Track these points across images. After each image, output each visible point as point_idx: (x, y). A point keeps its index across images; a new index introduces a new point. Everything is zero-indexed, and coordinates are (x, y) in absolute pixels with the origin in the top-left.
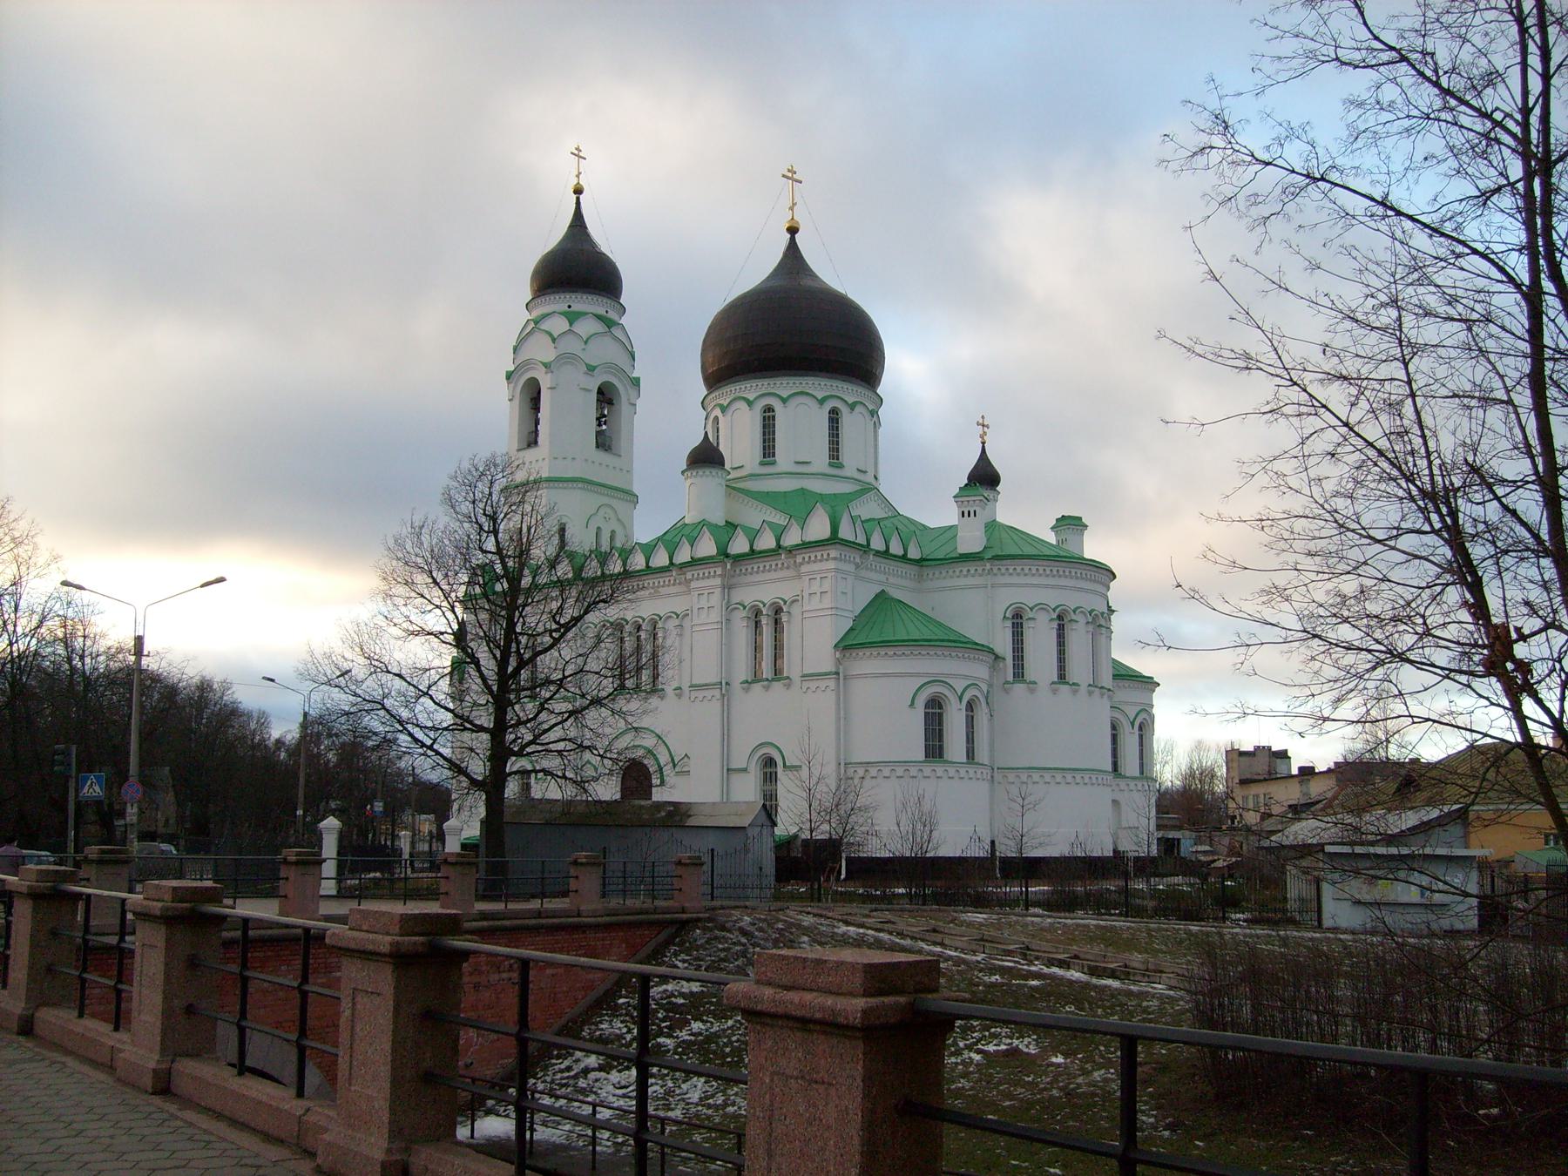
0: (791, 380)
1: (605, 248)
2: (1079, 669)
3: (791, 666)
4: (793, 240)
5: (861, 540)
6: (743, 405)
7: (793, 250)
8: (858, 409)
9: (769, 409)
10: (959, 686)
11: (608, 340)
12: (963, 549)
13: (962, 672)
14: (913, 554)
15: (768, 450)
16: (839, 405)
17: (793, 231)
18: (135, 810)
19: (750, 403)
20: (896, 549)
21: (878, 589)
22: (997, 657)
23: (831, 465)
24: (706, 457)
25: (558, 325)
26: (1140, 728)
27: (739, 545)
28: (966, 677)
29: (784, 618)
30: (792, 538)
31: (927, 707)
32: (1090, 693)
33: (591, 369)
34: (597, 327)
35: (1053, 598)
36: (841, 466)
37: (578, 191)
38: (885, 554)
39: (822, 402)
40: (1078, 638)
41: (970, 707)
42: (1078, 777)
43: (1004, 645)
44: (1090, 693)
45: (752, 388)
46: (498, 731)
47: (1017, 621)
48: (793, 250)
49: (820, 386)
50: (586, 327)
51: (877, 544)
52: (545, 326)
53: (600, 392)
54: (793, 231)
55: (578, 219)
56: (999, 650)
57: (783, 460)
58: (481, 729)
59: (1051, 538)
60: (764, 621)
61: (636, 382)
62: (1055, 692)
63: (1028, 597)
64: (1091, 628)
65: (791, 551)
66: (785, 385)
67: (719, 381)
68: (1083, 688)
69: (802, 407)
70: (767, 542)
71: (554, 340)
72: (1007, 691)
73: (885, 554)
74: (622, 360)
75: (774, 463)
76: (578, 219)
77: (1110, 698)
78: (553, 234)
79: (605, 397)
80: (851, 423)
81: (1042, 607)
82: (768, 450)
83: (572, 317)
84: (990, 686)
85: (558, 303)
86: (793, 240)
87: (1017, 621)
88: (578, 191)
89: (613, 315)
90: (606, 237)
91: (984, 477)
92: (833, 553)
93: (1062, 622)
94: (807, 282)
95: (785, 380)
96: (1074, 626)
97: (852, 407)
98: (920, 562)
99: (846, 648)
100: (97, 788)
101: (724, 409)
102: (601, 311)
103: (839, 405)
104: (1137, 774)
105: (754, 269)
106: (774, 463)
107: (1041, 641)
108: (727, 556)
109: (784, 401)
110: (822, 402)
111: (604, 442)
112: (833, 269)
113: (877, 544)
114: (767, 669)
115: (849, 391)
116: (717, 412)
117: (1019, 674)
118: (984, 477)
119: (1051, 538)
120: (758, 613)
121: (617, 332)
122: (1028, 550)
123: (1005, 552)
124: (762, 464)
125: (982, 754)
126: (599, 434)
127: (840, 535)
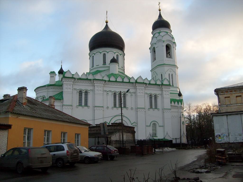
4: (107, 24)
6: (99, 53)
7: (107, 25)
8: (122, 55)
9: (104, 54)
16: (118, 54)
17: (107, 22)
19: (100, 53)
45: (101, 50)
48: (107, 25)
54: (107, 22)
66: (108, 49)
67: (94, 49)
69: (111, 53)
75: (106, 65)
86: (107, 24)
95: (108, 48)
97: (121, 55)
101: (95, 54)
103: (118, 54)
106: (106, 65)
116: (93, 55)
124: (103, 65)
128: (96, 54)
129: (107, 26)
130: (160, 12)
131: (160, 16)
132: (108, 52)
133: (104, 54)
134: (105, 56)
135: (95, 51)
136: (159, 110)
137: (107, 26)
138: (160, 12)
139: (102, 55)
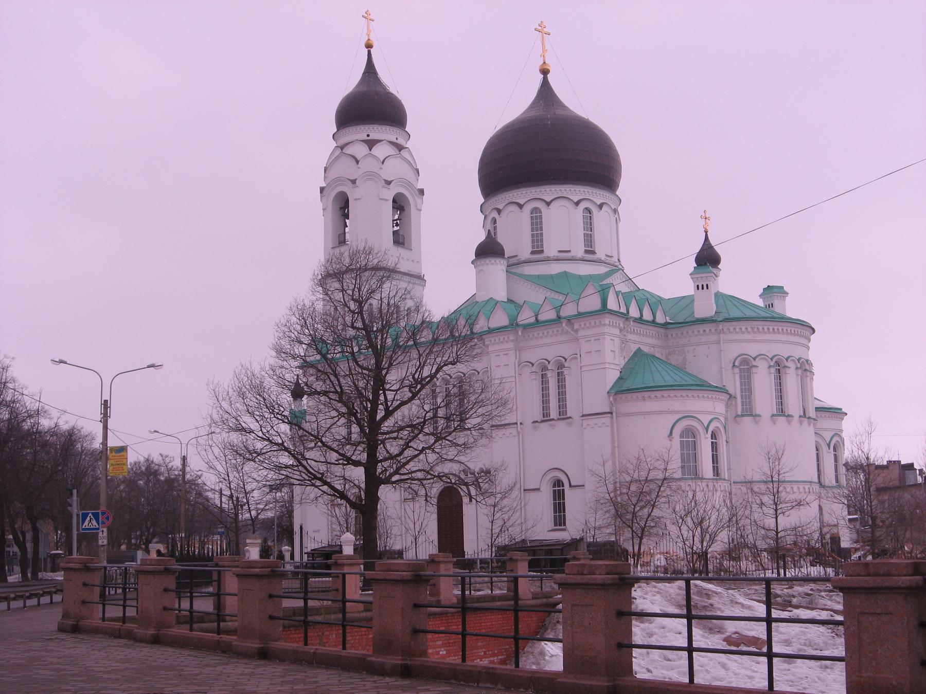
1: (392, 90)
2: (793, 406)
3: (572, 409)
5: (623, 310)
6: (515, 208)
8: (605, 208)
9: (536, 210)
10: (706, 419)
12: (699, 314)
13: (708, 409)
14: (660, 319)
17: (545, 72)
18: (105, 534)
19: (521, 206)
20: (647, 316)
22: (731, 396)
23: (586, 252)
24: (489, 249)
25: (360, 150)
26: (835, 450)
27: (526, 317)
28: (710, 413)
29: (566, 372)
30: (568, 311)
31: (682, 436)
32: (801, 423)
33: (389, 183)
34: (391, 150)
36: (593, 252)
37: (369, 46)
38: (640, 320)
40: (791, 379)
41: (714, 436)
44: (801, 423)
45: (522, 195)
46: (370, 466)
47: (745, 366)
49: (575, 192)
50: (381, 151)
51: (634, 312)
52: (349, 150)
53: (394, 201)
54: (545, 72)
55: (370, 69)
56: (731, 391)
58: (357, 464)
59: (760, 303)
60: (549, 374)
61: (421, 192)
62: (774, 422)
63: (752, 349)
64: (800, 372)
65: (569, 320)
66: (548, 192)
70: (548, 314)
71: (357, 162)
73: (640, 320)
74: (409, 175)
75: (542, 252)
76: (370, 69)
77: (814, 425)
78: (349, 81)
79: (399, 204)
80: (601, 219)
84: (726, 419)
85: (360, 132)
88: (369, 46)
89: (401, 141)
90: (392, 80)
91: (708, 258)
93: (779, 367)
94: (559, 112)
96: (787, 370)
97: (600, 207)
98: (665, 325)
99: (617, 393)
100: (94, 522)
101: (499, 211)
102: (395, 140)
104: (834, 483)
105: (513, 104)
107: (763, 381)
108: (517, 325)
111: (399, 240)
112: (579, 100)
113: (634, 312)
114: (554, 413)
115: (597, 195)
118: (708, 258)
119: (760, 303)
120: (544, 368)
121: (404, 153)
122: (749, 313)
123: (731, 315)
124: (532, 253)
125: (724, 473)
126: (395, 233)
127: (609, 307)
128: (503, 214)
132: (548, 204)
133: (536, 210)
134: (541, 217)
135: (501, 200)
139: (525, 215)
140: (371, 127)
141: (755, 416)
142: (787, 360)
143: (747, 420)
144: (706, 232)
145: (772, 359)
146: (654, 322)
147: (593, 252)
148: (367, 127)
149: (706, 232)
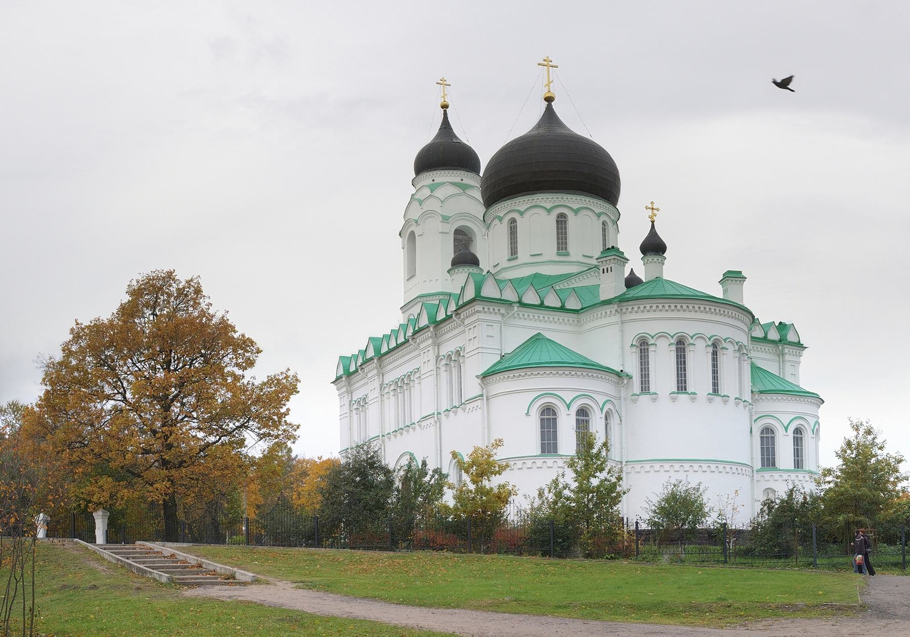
0: (526, 198)
1: (464, 141)
6: (497, 221)
9: (513, 221)
11: (464, 198)
15: (514, 251)
17: (549, 100)
19: (501, 219)
21: (533, 333)
22: (619, 375)
23: (558, 254)
33: (445, 219)
34: (456, 190)
35: (674, 328)
36: (568, 255)
39: (549, 211)
42: (728, 467)
43: (632, 367)
47: (643, 346)
54: (549, 100)
57: (523, 255)
62: (674, 400)
63: (651, 328)
66: (521, 203)
68: (732, 400)
72: (635, 401)
78: (428, 135)
81: (662, 335)
82: (514, 251)
83: (433, 187)
85: (428, 178)
87: (643, 346)
88: (445, 107)
92: (478, 307)
97: (576, 212)
102: (458, 180)
109: (522, 213)
110: (549, 211)
117: (645, 387)
129: (550, 115)
130: (445, 114)
131: (446, 125)
136: (693, 400)
137: (550, 115)
138: (445, 114)
140: (435, 173)
141: (655, 397)
142: (692, 338)
143: (645, 398)
144: (653, 222)
145: (709, 339)
146: (542, 306)
147: (568, 255)
148: (431, 173)
149: (653, 222)
